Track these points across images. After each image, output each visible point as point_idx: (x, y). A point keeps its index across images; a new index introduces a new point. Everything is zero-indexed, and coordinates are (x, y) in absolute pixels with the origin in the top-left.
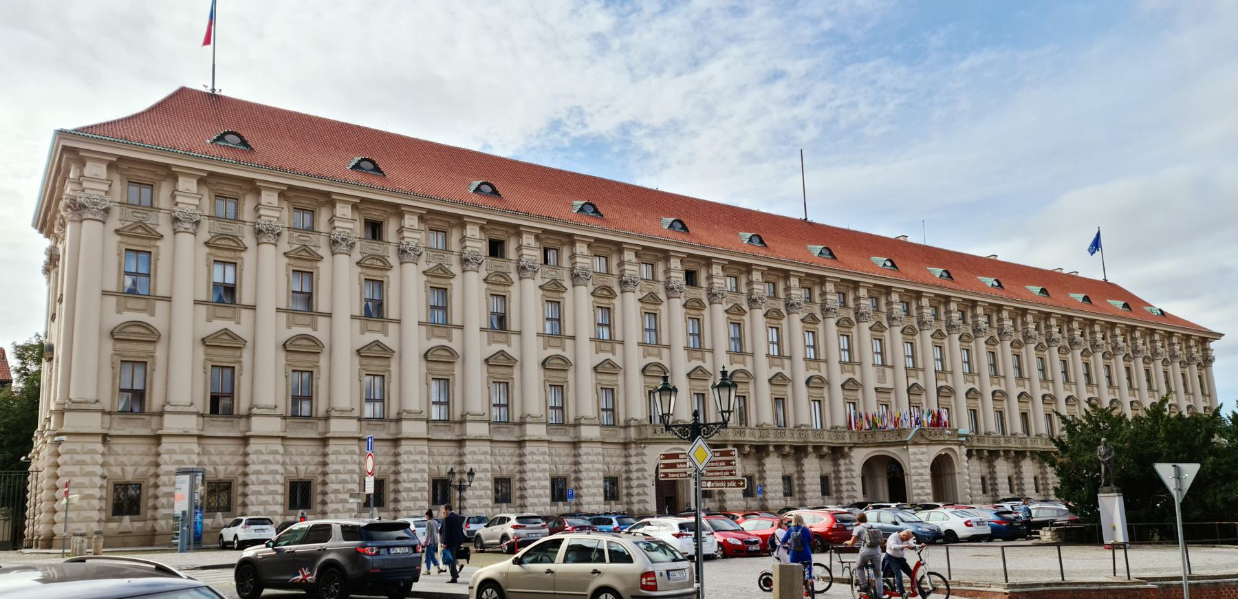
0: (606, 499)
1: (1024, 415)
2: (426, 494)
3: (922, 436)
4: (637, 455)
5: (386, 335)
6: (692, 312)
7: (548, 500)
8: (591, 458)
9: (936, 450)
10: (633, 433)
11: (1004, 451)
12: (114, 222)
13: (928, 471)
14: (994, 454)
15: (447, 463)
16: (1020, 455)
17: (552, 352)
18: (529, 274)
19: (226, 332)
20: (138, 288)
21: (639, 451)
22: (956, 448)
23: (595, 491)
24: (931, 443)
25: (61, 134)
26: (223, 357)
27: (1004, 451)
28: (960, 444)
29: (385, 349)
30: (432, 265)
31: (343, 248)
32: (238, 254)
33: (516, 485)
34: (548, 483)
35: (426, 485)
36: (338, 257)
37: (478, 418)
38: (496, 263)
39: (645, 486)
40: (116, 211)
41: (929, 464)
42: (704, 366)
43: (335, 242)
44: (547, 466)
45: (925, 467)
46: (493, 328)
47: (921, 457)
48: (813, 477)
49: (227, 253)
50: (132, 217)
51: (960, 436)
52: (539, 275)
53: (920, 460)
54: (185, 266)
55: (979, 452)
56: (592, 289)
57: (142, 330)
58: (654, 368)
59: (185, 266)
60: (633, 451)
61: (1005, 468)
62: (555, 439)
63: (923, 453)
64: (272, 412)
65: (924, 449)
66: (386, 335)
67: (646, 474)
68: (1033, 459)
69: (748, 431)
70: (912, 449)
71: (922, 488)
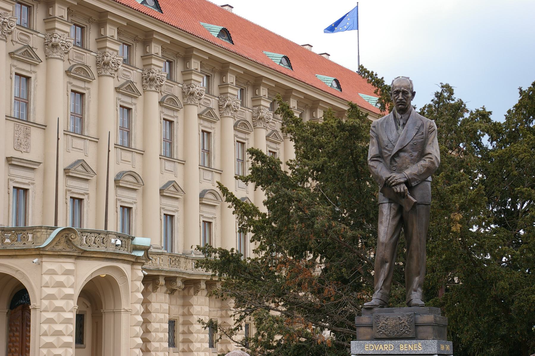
3: (69, 242)
9: (88, 270)
22: (126, 268)
24: (83, 255)
28: (135, 262)
41: (75, 292)
45: (68, 297)
47: (62, 278)
51: (136, 248)
53: (60, 285)
63: (67, 273)
65: (69, 265)
70: (49, 264)
71: (58, 333)
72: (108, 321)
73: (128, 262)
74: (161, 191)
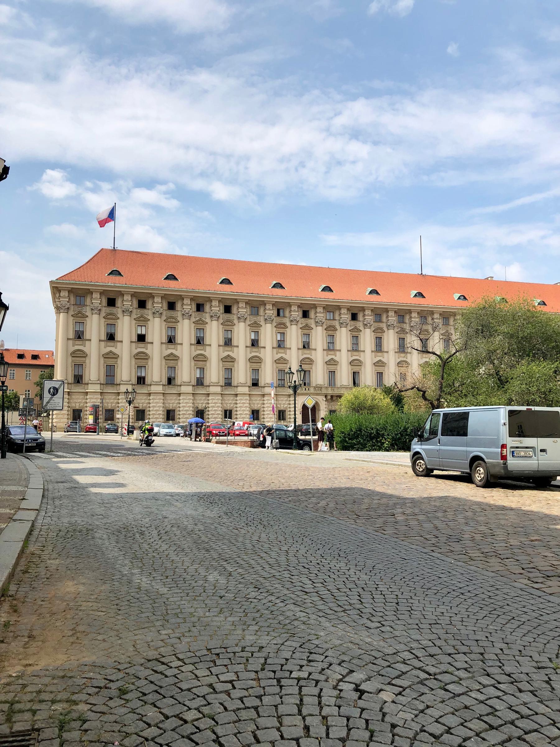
12: (71, 312)
19: (111, 352)
20: (79, 336)
25: (51, 282)
26: (110, 362)
30: (197, 319)
31: (157, 315)
32: (116, 321)
36: (155, 319)
38: (228, 315)
40: (72, 308)
43: (154, 313)
49: (111, 321)
50: (77, 309)
54: (95, 327)
57: (81, 353)
59: (95, 327)
64: (129, 383)
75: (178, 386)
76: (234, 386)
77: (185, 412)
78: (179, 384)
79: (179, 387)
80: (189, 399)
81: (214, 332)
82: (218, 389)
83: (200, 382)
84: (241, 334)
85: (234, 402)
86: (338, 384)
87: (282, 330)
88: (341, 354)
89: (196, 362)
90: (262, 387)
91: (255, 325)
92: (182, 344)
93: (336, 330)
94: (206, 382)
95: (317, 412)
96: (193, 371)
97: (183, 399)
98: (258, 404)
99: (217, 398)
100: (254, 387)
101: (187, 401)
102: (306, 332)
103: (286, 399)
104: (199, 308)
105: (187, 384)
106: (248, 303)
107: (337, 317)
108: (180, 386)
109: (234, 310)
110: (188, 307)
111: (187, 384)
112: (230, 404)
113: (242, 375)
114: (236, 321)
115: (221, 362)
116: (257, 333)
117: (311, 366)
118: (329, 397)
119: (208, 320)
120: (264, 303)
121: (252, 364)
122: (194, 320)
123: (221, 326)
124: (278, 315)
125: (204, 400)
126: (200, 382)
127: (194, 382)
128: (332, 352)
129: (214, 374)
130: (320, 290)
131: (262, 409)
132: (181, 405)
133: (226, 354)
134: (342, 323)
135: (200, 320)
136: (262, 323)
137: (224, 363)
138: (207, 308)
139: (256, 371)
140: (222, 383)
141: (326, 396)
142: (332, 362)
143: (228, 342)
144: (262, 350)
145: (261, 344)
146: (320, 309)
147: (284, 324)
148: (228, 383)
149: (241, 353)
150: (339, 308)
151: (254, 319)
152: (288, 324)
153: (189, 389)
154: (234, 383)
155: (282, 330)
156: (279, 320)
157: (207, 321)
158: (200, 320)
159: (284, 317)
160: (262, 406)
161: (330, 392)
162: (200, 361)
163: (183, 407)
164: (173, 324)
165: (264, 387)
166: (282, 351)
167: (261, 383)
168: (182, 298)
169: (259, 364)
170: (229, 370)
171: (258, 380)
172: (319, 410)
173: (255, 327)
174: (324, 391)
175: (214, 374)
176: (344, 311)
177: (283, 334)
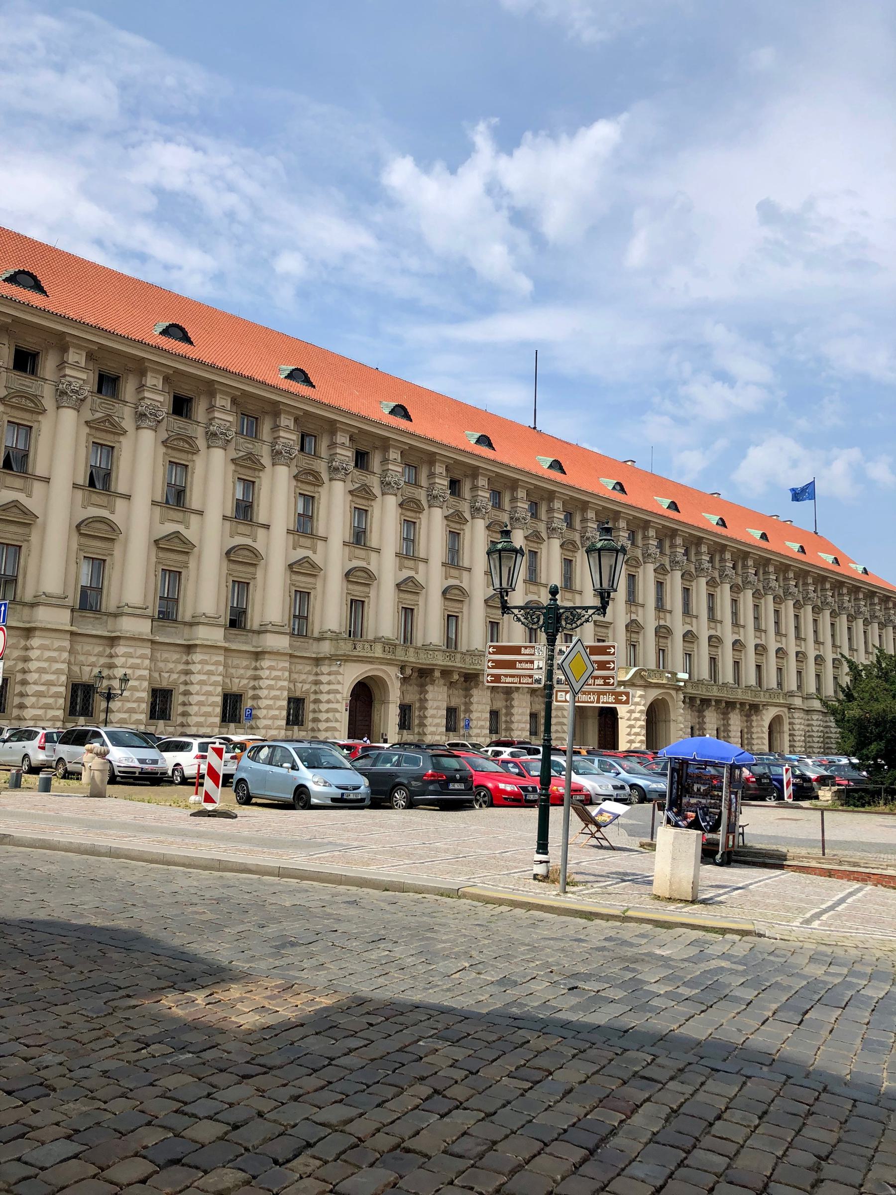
0: (287, 724)
1: (736, 664)
2: (61, 701)
4: (329, 674)
5: (29, 496)
6: (409, 513)
7: (217, 720)
8: (275, 673)
10: (326, 648)
11: (716, 701)
13: (644, 717)
14: (706, 702)
15: (93, 665)
16: (730, 705)
17: (239, 540)
18: (220, 443)
21: (334, 668)
22: (673, 693)
23: (277, 712)
27: (716, 701)
29: (26, 512)
30: (98, 415)
33: (178, 698)
34: (219, 699)
35: (62, 689)
37: (139, 612)
38: (178, 423)
39: (336, 711)
42: (416, 576)
44: (220, 678)
46: (167, 502)
48: (522, 714)
52: (232, 445)
55: (692, 699)
56: (295, 471)
58: (359, 574)
60: (325, 669)
61: (714, 720)
62: (234, 646)
66: (29, 496)
67: (339, 696)
68: (741, 710)
69: (458, 656)
72: (662, 726)
73: (674, 689)
74: (684, 636)
75: (25, 604)
76: (185, 623)
77: (43, 688)
78: (28, 597)
79: (26, 610)
80: (60, 649)
81: (141, 460)
82: (143, 627)
83: (89, 602)
84: (213, 479)
85: (181, 667)
86: (419, 641)
87: (308, 490)
88: (427, 567)
89: (84, 540)
90: (254, 632)
91: (248, 463)
92: (47, 480)
93: (419, 509)
94: (110, 602)
95: (376, 705)
96: (73, 567)
97: (42, 647)
98: (241, 677)
99: (140, 652)
100: (234, 631)
101: (54, 654)
102: (362, 503)
103: (308, 668)
104: (108, 384)
105: (55, 602)
106: (239, 401)
107: (424, 482)
108: (33, 605)
109: (200, 410)
110: (80, 375)
111: (55, 602)
112: (171, 671)
113: (206, 592)
114: (201, 443)
115: (154, 549)
116: (249, 485)
117: (366, 589)
118: (408, 672)
119: (128, 423)
120: (275, 410)
121: (233, 566)
122: (89, 416)
123: (162, 450)
124: (302, 449)
125: (99, 655)
126: (89, 602)
127: (73, 599)
128: (410, 563)
129: (133, 580)
130: (387, 411)
131: (251, 693)
132: (33, 665)
133: (170, 527)
134: (435, 497)
135: (108, 418)
136: (266, 460)
137: (161, 555)
138: (129, 389)
139: (242, 587)
140: (153, 609)
141: (402, 669)
142: (410, 586)
143: (176, 498)
144: (261, 532)
145: (261, 516)
146: (394, 455)
147: (316, 475)
148: (167, 612)
149: (210, 533)
150: (431, 459)
151: (247, 446)
152: (325, 476)
153: (61, 618)
154: (186, 612)
155: (308, 490)
156: (305, 462)
157: (124, 424)
158: (108, 418)
159: (316, 456)
160: (252, 683)
161: (411, 657)
162: (96, 538)
163: (41, 671)
164: (27, 416)
165: (259, 632)
166: (307, 542)
167: (254, 620)
168: (62, 343)
169: (251, 569)
170: (173, 576)
171: (244, 612)
172: (385, 702)
173: (247, 471)
174: (400, 655)
175: (133, 580)
176: (440, 469)
177: (309, 499)
